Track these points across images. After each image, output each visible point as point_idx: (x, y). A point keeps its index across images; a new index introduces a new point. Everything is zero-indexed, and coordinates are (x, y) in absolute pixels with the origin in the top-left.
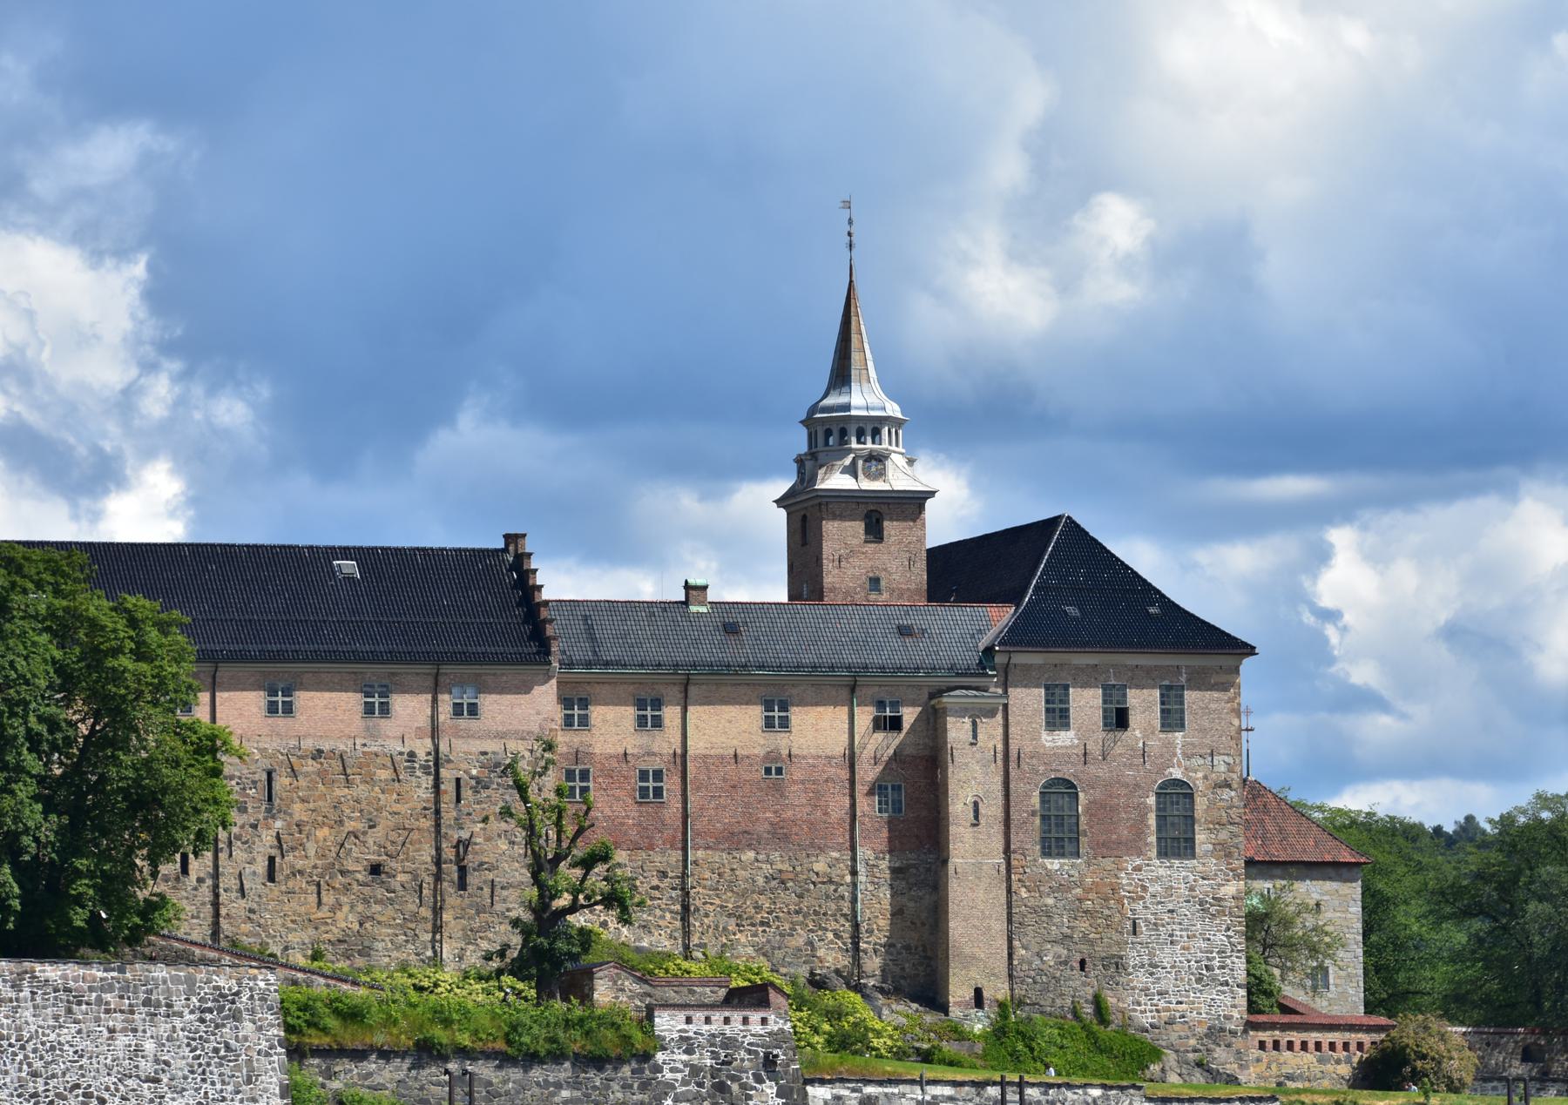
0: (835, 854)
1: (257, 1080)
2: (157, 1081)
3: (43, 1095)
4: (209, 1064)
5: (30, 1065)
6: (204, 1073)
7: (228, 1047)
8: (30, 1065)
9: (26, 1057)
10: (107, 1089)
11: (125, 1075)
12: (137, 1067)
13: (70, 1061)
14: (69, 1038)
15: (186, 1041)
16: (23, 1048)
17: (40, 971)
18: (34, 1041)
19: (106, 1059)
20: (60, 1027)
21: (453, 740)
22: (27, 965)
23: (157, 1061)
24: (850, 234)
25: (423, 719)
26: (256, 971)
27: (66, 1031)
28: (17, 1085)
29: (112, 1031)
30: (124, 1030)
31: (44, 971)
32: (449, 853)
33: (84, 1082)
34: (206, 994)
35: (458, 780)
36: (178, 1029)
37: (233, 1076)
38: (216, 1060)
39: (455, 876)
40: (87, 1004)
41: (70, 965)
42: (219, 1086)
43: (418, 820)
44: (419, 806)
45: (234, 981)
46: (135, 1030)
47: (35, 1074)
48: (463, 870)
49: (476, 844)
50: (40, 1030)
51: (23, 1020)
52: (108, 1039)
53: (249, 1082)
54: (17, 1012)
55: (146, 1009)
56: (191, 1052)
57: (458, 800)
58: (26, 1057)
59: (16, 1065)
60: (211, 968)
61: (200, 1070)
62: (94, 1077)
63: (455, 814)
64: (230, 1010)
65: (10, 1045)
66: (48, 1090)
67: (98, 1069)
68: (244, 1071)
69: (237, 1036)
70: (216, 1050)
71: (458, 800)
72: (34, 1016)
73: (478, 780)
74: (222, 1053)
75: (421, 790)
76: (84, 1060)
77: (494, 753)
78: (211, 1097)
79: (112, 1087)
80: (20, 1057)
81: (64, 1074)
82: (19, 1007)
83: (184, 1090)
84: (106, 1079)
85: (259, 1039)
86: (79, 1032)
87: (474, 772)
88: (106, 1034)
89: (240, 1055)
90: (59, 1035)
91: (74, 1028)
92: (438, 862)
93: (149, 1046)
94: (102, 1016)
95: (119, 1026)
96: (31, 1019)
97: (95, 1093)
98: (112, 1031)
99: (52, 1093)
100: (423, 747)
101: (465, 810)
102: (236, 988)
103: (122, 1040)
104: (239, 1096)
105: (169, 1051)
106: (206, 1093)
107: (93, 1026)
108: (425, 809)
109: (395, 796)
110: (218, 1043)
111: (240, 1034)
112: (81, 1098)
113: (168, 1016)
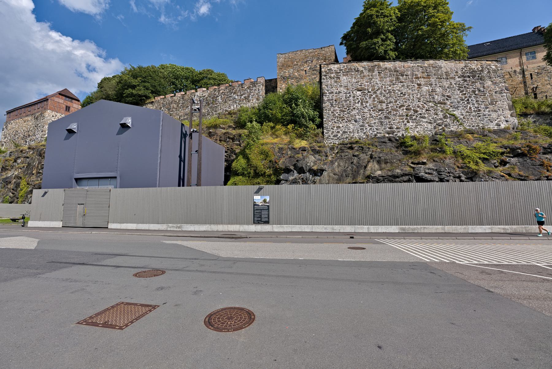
1: (496, 103)
2: (445, 104)
3: (386, 110)
4: (470, 97)
5: (378, 99)
6: (468, 100)
7: (479, 90)
8: (378, 99)
9: (377, 96)
10: (419, 107)
12: (434, 98)
13: (398, 97)
14: (398, 88)
16: (375, 93)
17: (382, 65)
18: (381, 90)
19: (417, 95)
20: (393, 84)
21: (528, 65)
22: (376, 63)
23: (443, 96)
26: (490, 62)
27: (396, 86)
28: (372, 106)
29: (419, 85)
30: (426, 85)
31: (385, 65)
32: (530, 90)
35: (531, 74)
36: (453, 84)
37: (484, 101)
38: (474, 95)
39: (533, 96)
40: (406, 75)
42: (476, 105)
43: (519, 85)
45: (479, 66)
46: (431, 85)
47: (381, 102)
48: (535, 94)
49: (539, 87)
50: (384, 86)
51: (375, 83)
52: (418, 88)
53: (492, 104)
54: (372, 80)
55: (436, 76)
56: (460, 92)
57: (532, 78)
58: (377, 96)
59: (372, 99)
60: (467, 61)
61: (466, 99)
62: (412, 102)
63: (531, 82)
64: (479, 76)
65: (369, 92)
66: (388, 108)
67: (413, 99)
68: (489, 99)
71: (532, 78)
72: (380, 81)
73: (538, 73)
74: (477, 92)
75: (520, 78)
76: (406, 96)
77: (543, 66)
78: (473, 110)
79: (421, 106)
81: (396, 102)
82: (373, 78)
83: (458, 107)
85: (495, 87)
87: (536, 71)
88: (416, 86)
89: (485, 94)
90: (393, 88)
91: (400, 85)
92: (526, 93)
94: (414, 80)
95: (423, 83)
96: (379, 82)
98: (419, 85)
99: (390, 109)
100: (518, 69)
102: (481, 69)
103: (425, 88)
104: (487, 110)
105: (449, 92)
106: (470, 108)
107: (410, 84)
108: (521, 82)
109: (511, 81)
111: (485, 85)
112: (405, 110)
113: (448, 79)
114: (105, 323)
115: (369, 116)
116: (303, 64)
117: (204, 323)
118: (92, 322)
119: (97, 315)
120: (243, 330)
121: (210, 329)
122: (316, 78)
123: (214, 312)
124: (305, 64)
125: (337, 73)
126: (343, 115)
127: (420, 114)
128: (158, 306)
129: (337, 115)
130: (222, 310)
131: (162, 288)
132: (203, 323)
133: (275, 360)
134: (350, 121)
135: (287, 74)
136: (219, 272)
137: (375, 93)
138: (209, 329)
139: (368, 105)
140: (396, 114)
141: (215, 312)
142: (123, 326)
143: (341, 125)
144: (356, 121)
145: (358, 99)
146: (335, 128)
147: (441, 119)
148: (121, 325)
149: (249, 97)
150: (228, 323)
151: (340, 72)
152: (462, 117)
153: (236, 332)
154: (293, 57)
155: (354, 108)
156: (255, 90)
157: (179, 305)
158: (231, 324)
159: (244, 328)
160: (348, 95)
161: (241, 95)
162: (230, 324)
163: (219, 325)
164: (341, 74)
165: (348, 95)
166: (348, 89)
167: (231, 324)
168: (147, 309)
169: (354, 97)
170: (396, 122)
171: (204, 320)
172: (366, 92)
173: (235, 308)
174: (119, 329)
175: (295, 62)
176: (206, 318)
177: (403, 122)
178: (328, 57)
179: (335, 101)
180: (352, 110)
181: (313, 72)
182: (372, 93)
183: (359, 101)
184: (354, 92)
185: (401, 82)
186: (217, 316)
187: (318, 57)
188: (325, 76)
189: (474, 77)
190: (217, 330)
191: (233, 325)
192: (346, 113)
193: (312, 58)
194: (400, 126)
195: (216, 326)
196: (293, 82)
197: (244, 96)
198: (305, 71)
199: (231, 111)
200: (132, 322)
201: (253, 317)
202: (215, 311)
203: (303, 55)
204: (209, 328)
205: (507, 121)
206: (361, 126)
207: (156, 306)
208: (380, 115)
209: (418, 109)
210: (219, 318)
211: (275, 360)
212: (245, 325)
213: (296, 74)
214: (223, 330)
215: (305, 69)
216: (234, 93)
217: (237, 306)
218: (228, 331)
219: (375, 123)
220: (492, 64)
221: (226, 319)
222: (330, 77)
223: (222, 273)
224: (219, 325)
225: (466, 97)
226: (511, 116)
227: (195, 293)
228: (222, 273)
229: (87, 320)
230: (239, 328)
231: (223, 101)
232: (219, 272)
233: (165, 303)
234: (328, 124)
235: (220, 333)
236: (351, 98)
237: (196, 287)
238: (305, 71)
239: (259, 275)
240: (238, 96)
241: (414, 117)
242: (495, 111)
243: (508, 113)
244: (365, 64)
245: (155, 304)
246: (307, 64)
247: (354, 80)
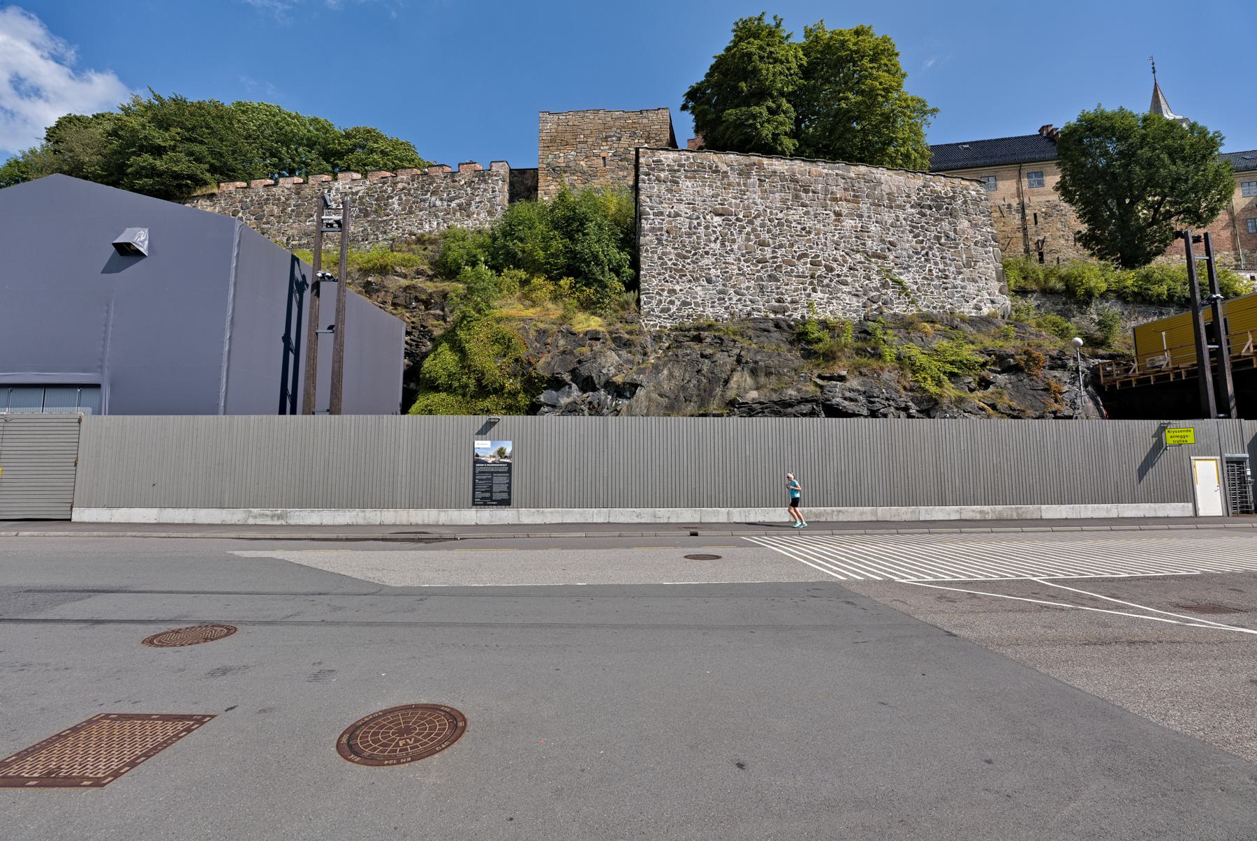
0: (1227, 253)
1: (975, 265)
2: (885, 258)
3: (771, 261)
4: (931, 248)
5: (757, 236)
6: (927, 254)
7: (948, 237)
8: (757, 236)
9: (754, 230)
10: (835, 260)
11: (852, 250)
12: (864, 244)
13: (797, 235)
14: (797, 217)
15: (908, 228)
16: (750, 222)
18: (762, 218)
19: (834, 236)
20: (787, 208)
23: (883, 241)
24: (1153, 68)
25: (1014, 190)
26: (968, 183)
27: (792, 212)
28: (744, 251)
29: (838, 214)
30: (850, 215)
31: (772, 165)
32: (1032, 247)
33: (811, 253)
34: (925, 194)
35: (1035, 215)
36: (901, 219)
37: (954, 260)
38: (938, 245)
39: (1038, 257)
40: (814, 192)
41: (797, 161)
42: (941, 266)
44: (1015, 227)
45: (949, 189)
46: (860, 216)
47: (763, 244)
48: (1041, 254)
50: (768, 211)
51: (751, 201)
52: (835, 220)
53: (968, 265)
54: (745, 194)
56: (914, 237)
57: (1036, 223)
58: (754, 230)
59: (744, 236)
60: (928, 176)
61: (924, 252)
62: (822, 250)
63: (1035, 229)
64: (947, 208)
65: (738, 220)
67: (825, 243)
68: (964, 256)
69: (955, 229)
70: (938, 238)
71: (1036, 223)
72: (762, 199)
74: (943, 241)
75: (1016, 220)
76: (812, 236)
78: (935, 274)
79: (840, 259)
80: (748, 229)
81: (792, 245)
82: (748, 191)
83: (909, 266)
84: (834, 252)
85: (975, 233)
86: (807, 213)
87: (1044, 210)
88: (833, 217)
89: (958, 244)
90: (788, 215)
91: (801, 210)
92: (1027, 251)
93: (873, 228)
94: (829, 202)
95: (845, 211)
97: (823, 262)
98: (838, 214)
99: (780, 260)
100: (1015, 203)
101: (1040, 227)
103: (848, 223)
104: (961, 277)
105: (893, 235)
106: (930, 271)
107: (820, 210)
110: (939, 232)
111: (958, 228)
112: (809, 265)
113: (891, 207)
114: (49, 773)
115: (736, 271)
116: (598, 143)
117: (337, 747)
120: (436, 756)
123: (363, 719)
124: (604, 144)
125: (672, 170)
126: (684, 266)
127: (839, 276)
128: (213, 717)
129: (670, 263)
130: (385, 712)
131: (225, 671)
132: (334, 749)
133: (511, 819)
134: (697, 280)
135: (561, 160)
136: (380, 624)
137: (750, 222)
138: (349, 763)
139: (735, 247)
140: (792, 271)
141: (367, 719)
142: (105, 778)
143: (677, 288)
144: (709, 281)
145: (714, 232)
147: (876, 289)
149: (469, 205)
150: (398, 743)
151: (679, 171)
152: (915, 287)
153: (417, 764)
154: (576, 123)
155: (707, 253)
156: (485, 190)
157: (271, 709)
158: (407, 744)
159: (437, 752)
160: (695, 222)
161: (451, 200)
162: (404, 745)
163: (375, 749)
164: (682, 174)
165: (695, 222)
166: (694, 210)
167: (407, 744)
168: (180, 726)
169: (707, 228)
170: (791, 288)
171: (336, 742)
172: (733, 218)
173: (417, 707)
174: (90, 786)
175: (582, 136)
176: (342, 736)
177: (805, 290)
178: (656, 134)
179: (667, 232)
180: (702, 256)
181: (620, 163)
182: (744, 223)
183: (717, 238)
184: (708, 217)
185: (804, 205)
186: (372, 728)
187: (633, 130)
188: (647, 174)
189: (939, 208)
190: (370, 762)
191: (411, 748)
192: (689, 261)
193: (618, 131)
194: (797, 298)
195: (368, 752)
196: (575, 180)
198: (604, 158)
199: (423, 235)
200: (133, 764)
201: (461, 724)
202: (368, 717)
203: (600, 121)
205: (993, 302)
206: (720, 292)
207: (205, 717)
208: (758, 271)
209: (835, 265)
211: (511, 819)
212: (440, 746)
213: (582, 163)
214: (386, 762)
215: (603, 154)
216: (433, 193)
217: (424, 701)
218: (399, 763)
219: (748, 288)
220: (971, 188)
221: (393, 734)
222: (658, 179)
224: (375, 749)
225: (923, 248)
226: (1000, 291)
227: (316, 677)
228: (390, 624)
230: (425, 754)
231: (404, 209)
232: (380, 624)
233: (231, 708)
234: (650, 282)
236: (701, 230)
237: (320, 663)
238: (604, 158)
239: (482, 625)
240: (441, 200)
241: (826, 281)
242: (974, 281)
243: (995, 285)
244: (732, 157)
245: (203, 713)
246: (609, 143)
247: (708, 191)
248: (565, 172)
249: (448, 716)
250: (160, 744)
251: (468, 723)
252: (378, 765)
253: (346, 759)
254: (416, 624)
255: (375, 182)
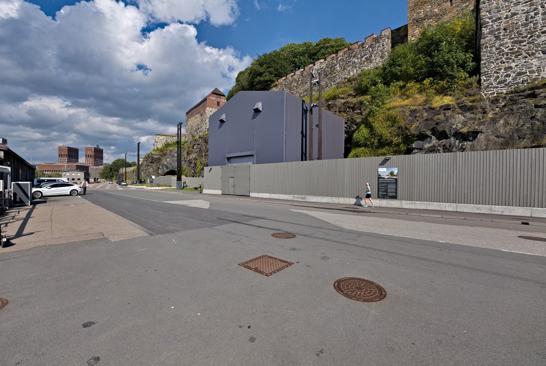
114: (256, 268)
117: (334, 287)
118: (247, 266)
119: (251, 261)
120: (374, 303)
121: (340, 294)
122: (469, 6)
123: (342, 279)
128: (293, 264)
130: (351, 279)
131: (294, 249)
132: (333, 287)
133: (414, 344)
136: (344, 243)
138: (339, 294)
141: (343, 279)
142: (269, 274)
143: (513, 65)
146: (503, 71)
148: (267, 273)
149: (371, 56)
150: (357, 292)
153: (366, 303)
157: (309, 266)
158: (360, 294)
159: (374, 301)
161: (362, 58)
162: (359, 294)
163: (348, 292)
167: (360, 294)
168: (285, 264)
171: (333, 284)
173: (363, 280)
174: (265, 275)
176: (335, 283)
179: (505, 29)
186: (346, 283)
190: (347, 296)
191: (363, 296)
195: (345, 292)
197: (365, 57)
199: (350, 78)
200: (274, 272)
201: (384, 293)
202: (344, 278)
204: (339, 293)
207: (291, 263)
210: (347, 286)
211: (414, 344)
212: (375, 299)
213: (436, 10)
214: (353, 298)
216: (354, 57)
217: (366, 278)
218: (358, 300)
221: (355, 288)
223: (348, 244)
224: (348, 292)
227: (324, 258)
228: (348, 244)
229: (244, 264)
230: (369, 301)
231: (341, 69)
232: (344, 243)
233: (298, 262)
235: (350, 300)
237: (324, 253)
239: (388, 252)
240: (358, 59)
245: (290, 262)
248: (425, 19)
249: (377, 288)
250: (283, 267)
251: (387, 294)
252: (350, 298)
253: (338, 292)
254: (358, 246)
255: (329, 60)
